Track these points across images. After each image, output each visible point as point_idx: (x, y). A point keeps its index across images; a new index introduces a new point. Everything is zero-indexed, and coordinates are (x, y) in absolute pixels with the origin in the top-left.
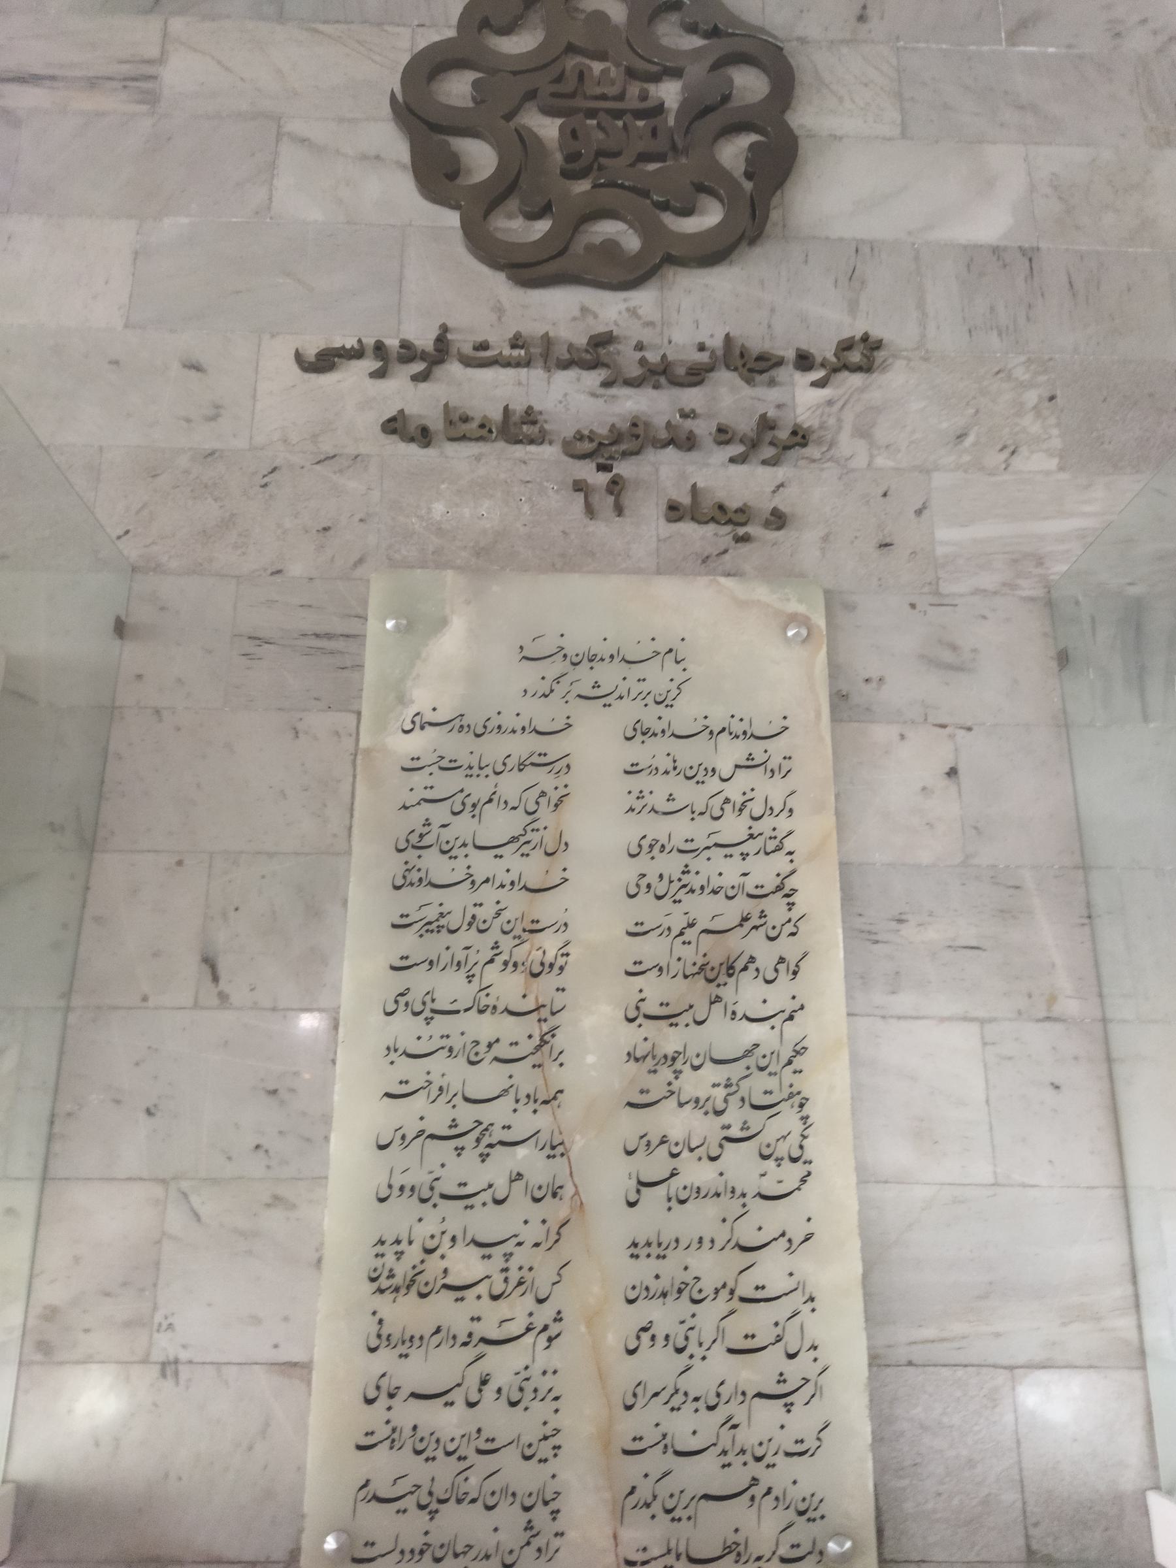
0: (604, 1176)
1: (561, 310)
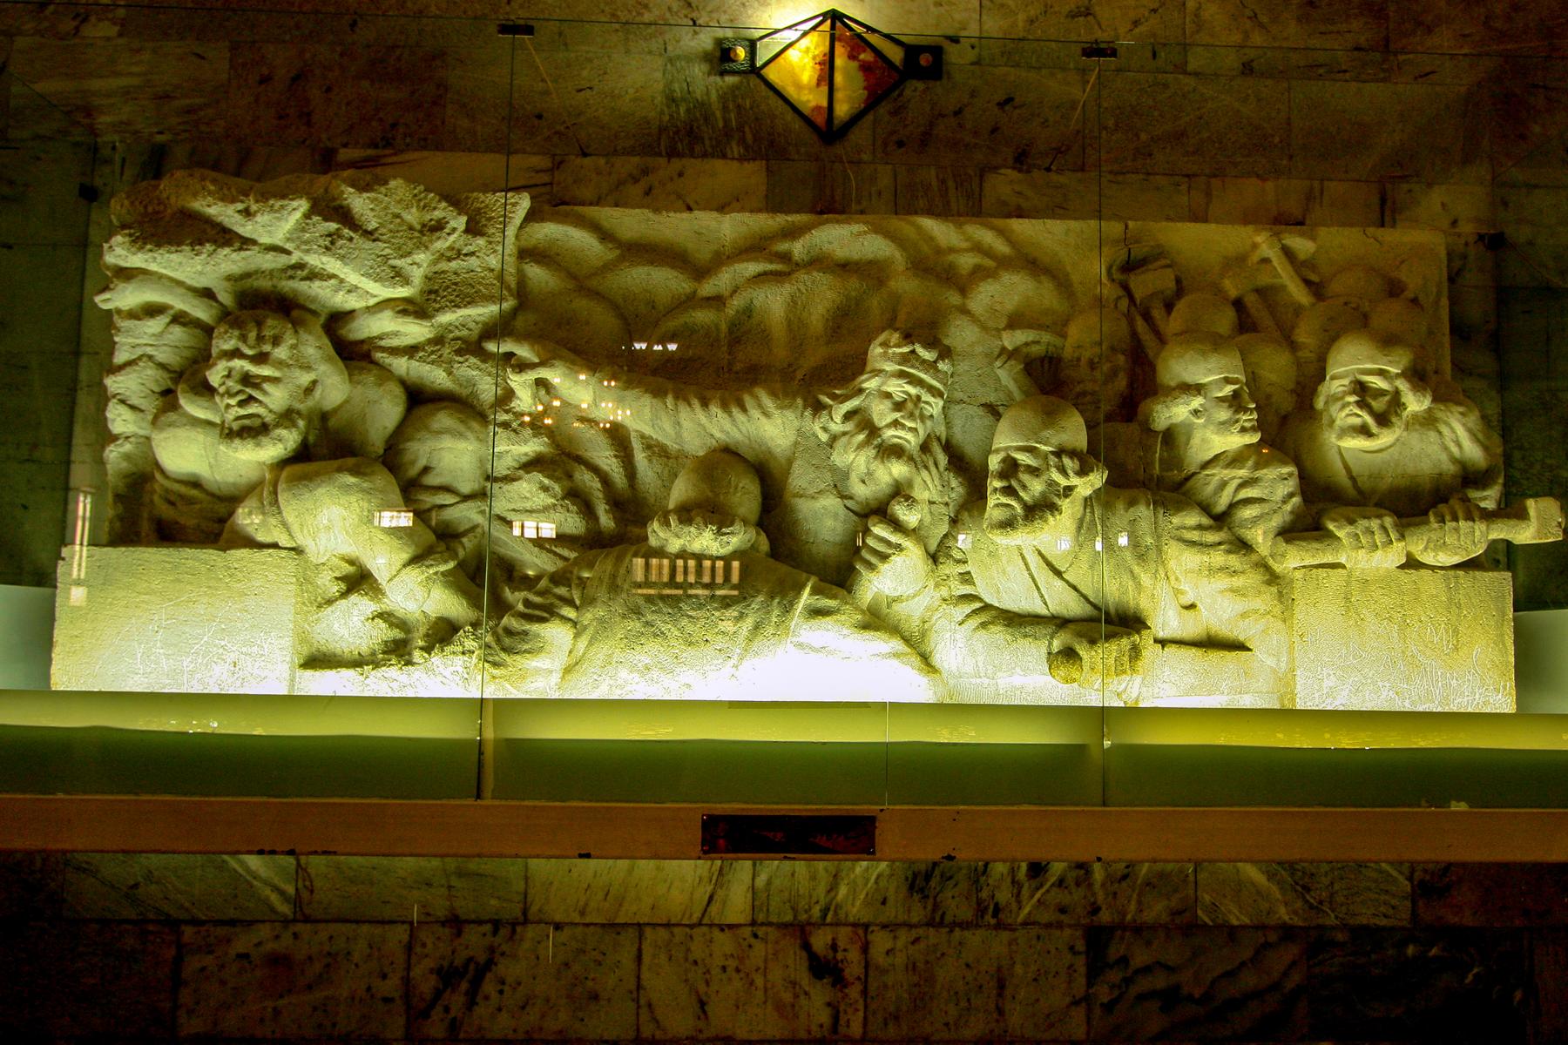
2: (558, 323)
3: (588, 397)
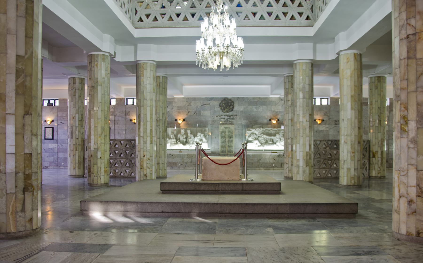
0: (227, 144)
1: (225, 114)
2: (264, 133)
3: (265, 136)
